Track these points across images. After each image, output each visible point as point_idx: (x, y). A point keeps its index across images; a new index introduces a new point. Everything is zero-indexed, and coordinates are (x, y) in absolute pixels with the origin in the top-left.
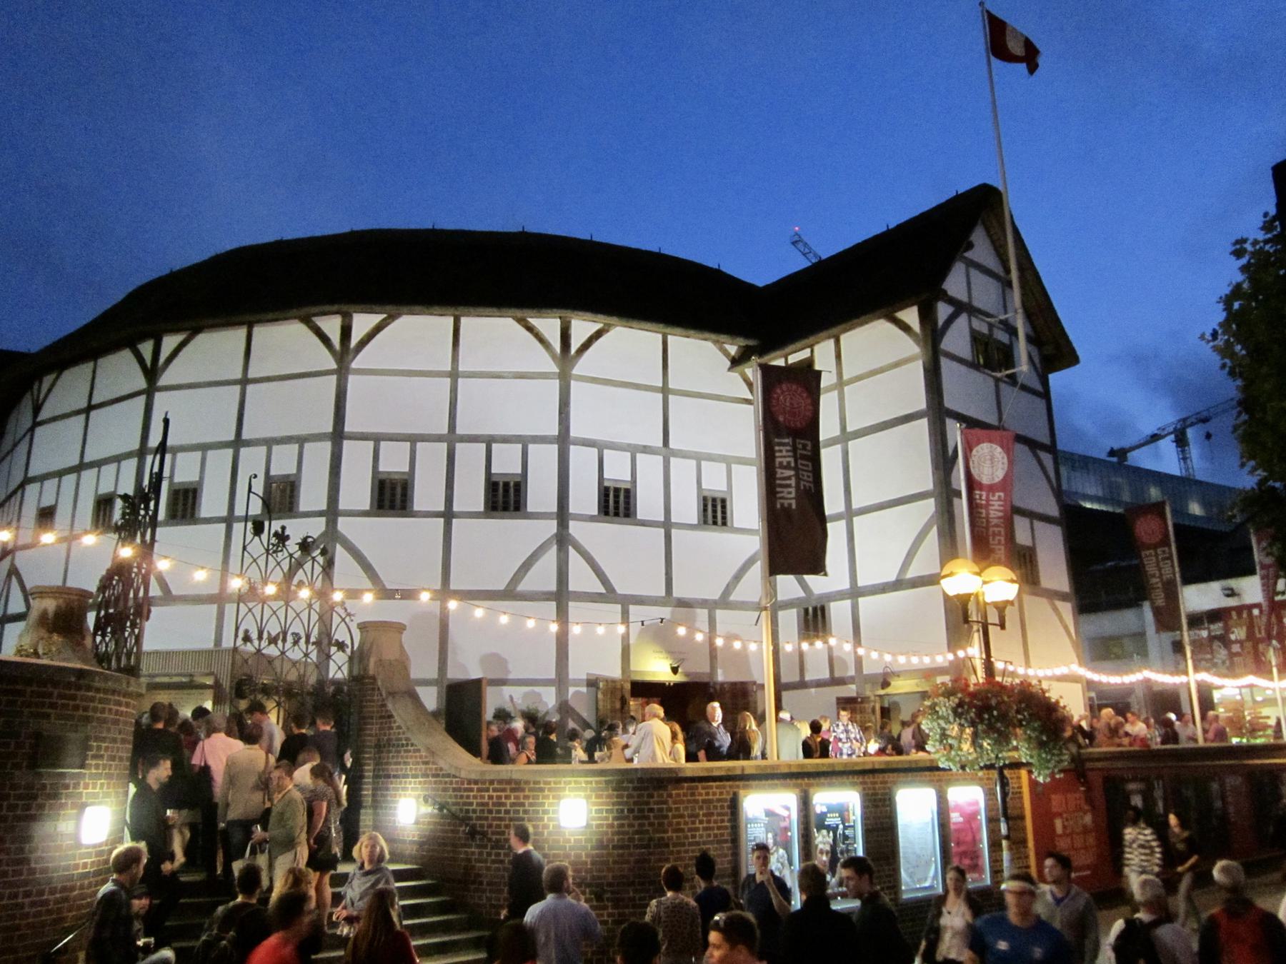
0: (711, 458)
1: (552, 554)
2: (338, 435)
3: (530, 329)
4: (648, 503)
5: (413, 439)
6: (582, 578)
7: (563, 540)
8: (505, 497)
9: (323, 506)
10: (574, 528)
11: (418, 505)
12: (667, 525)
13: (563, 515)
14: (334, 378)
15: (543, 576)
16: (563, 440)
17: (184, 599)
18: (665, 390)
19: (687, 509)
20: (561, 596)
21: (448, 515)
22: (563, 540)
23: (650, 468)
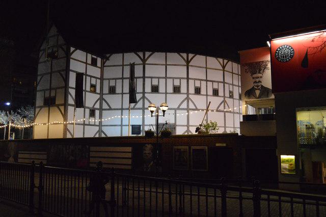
0: (215, 81)
1: (186, 101)
2: (144, 77)
3: (180, 55)
4: (203, 91)
5: (159, 78)
6: (191, 106)
7: (188, 99)
8: (177, 90)
9: (142, 91)
10: (190, 96)
11: (160, 91)
12: (207, 95)
13: (188, 93)
14: (142, 66)
15: (184, 106)
16: (188, 79)
17: (115, 109)
18: (206, 68)
19: (210, 92)
20: (188, 109)
21: (166, 93)
22: (188, 99)
23: (204, 83)
